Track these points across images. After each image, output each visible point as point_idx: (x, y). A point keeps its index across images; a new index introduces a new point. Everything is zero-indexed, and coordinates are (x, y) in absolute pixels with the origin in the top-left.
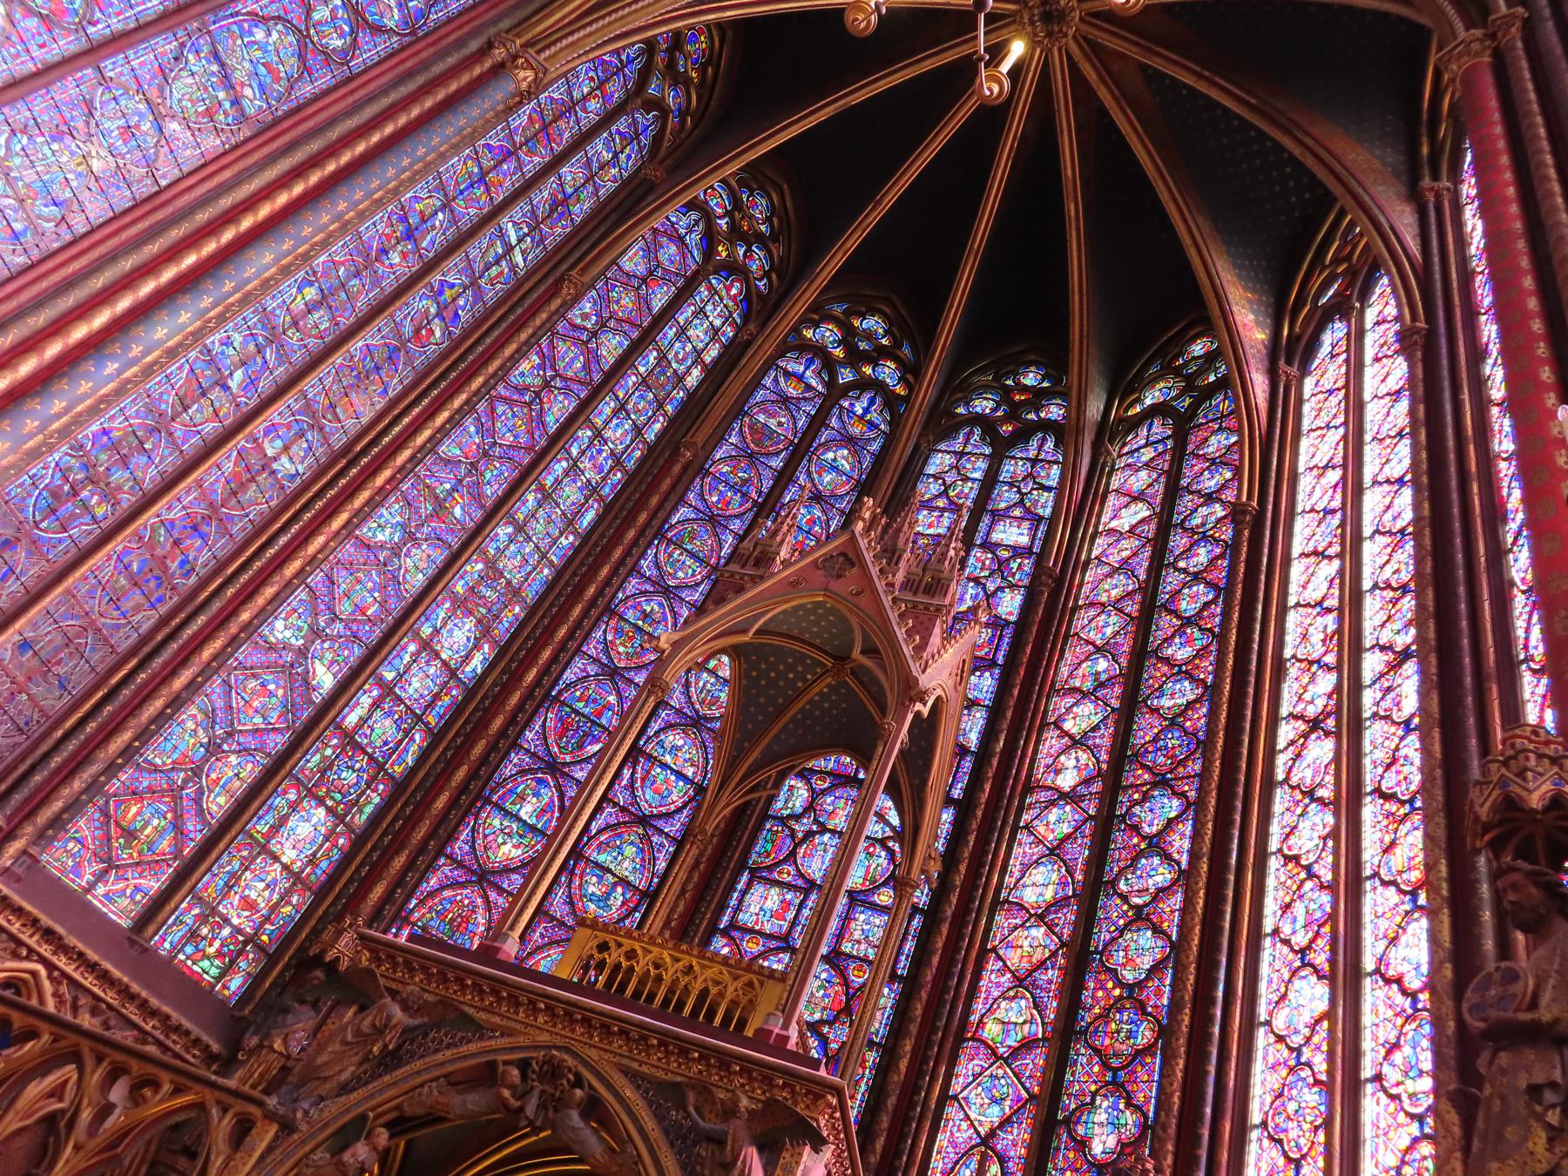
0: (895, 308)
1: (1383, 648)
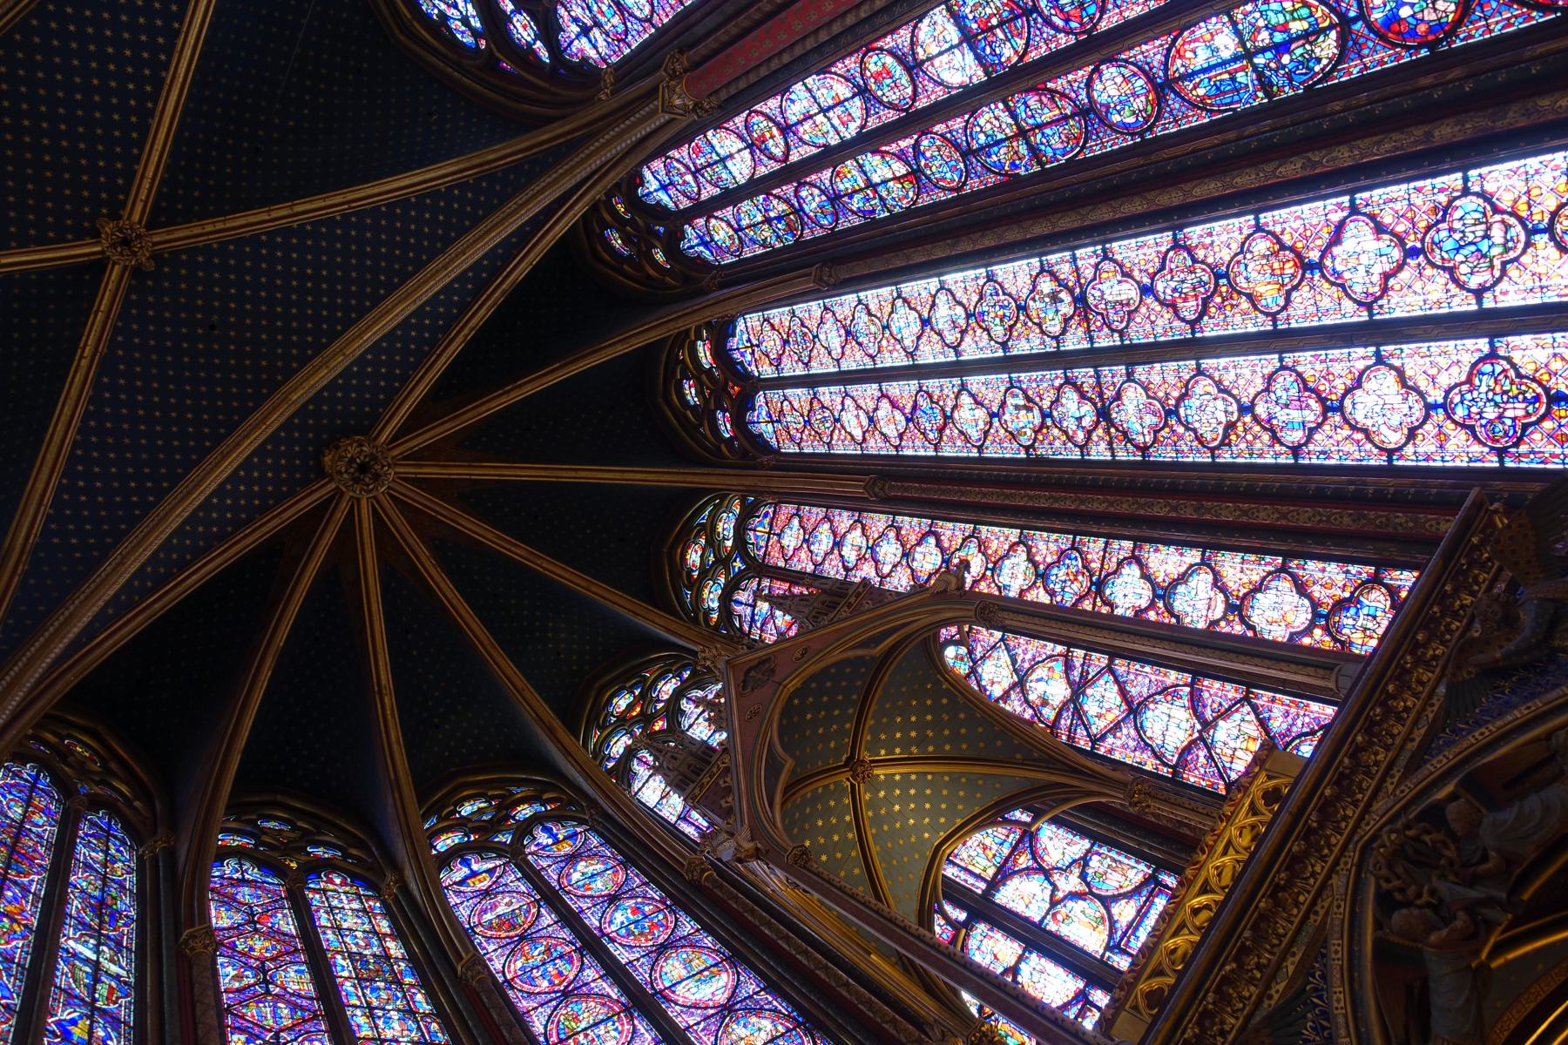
1: (1064, 332)
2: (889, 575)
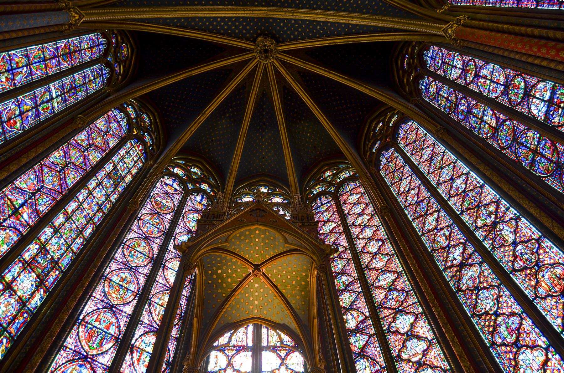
1: (481, 228)
2: (359, 239)
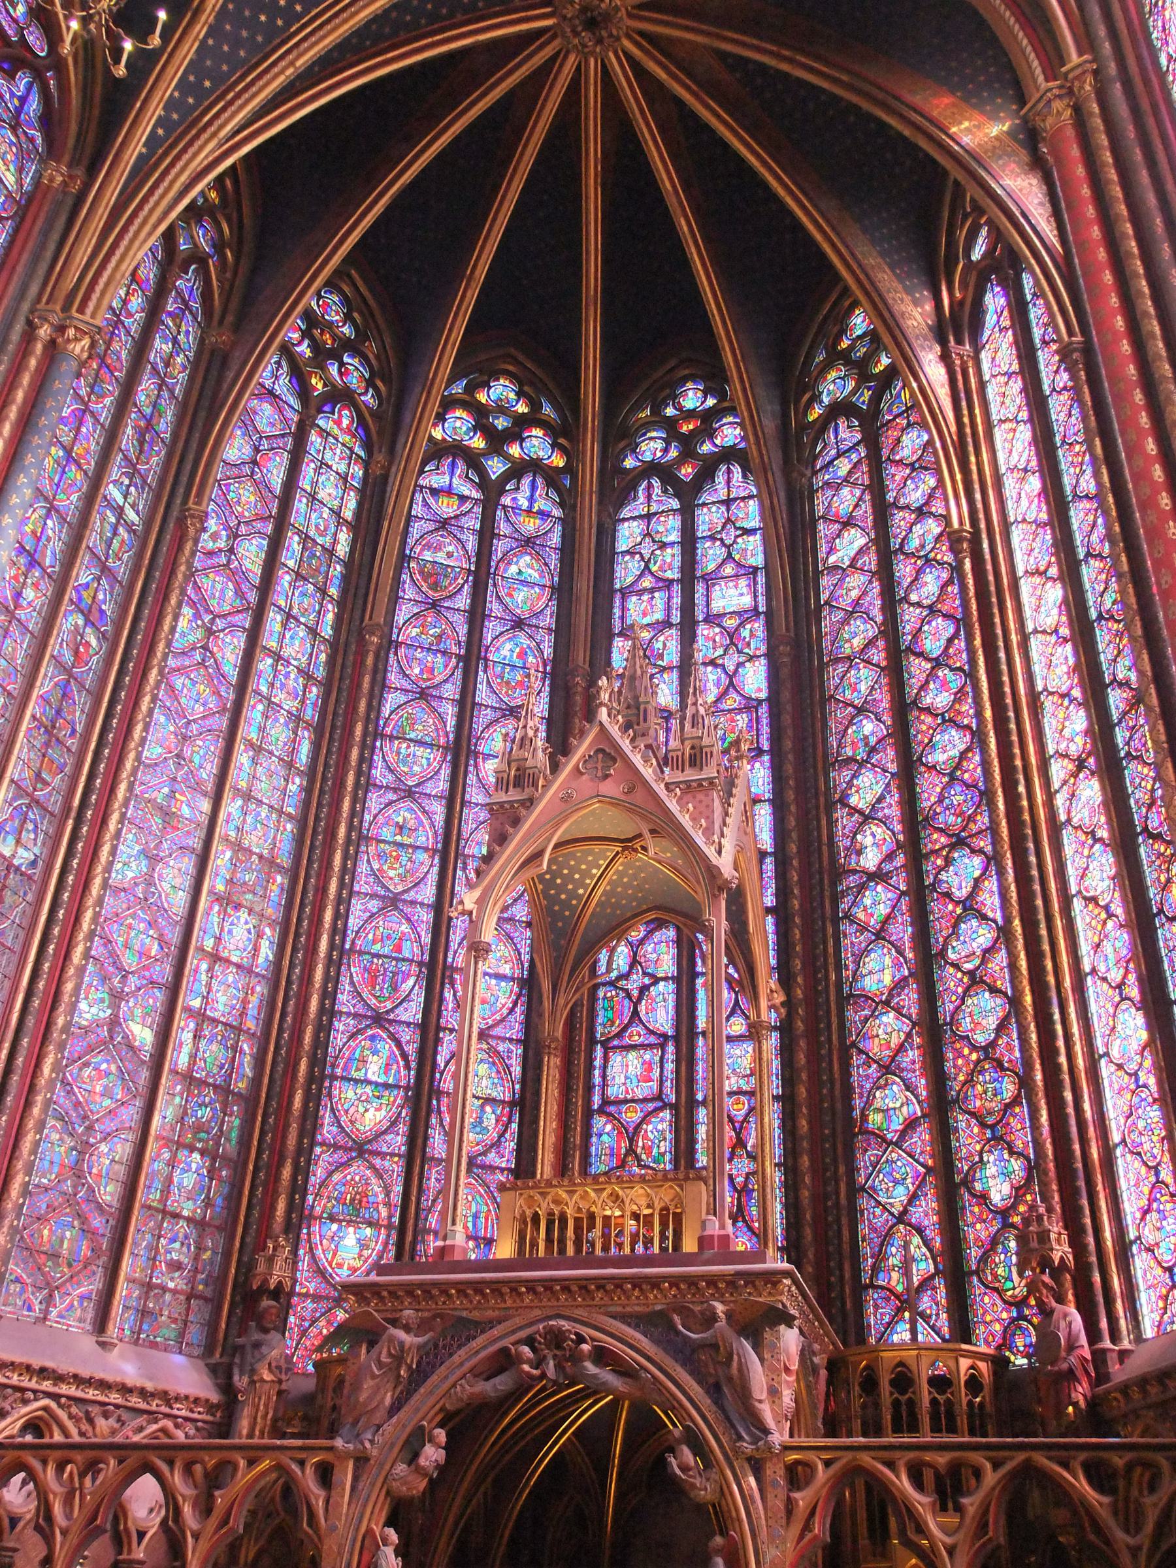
0: (516, 362)
